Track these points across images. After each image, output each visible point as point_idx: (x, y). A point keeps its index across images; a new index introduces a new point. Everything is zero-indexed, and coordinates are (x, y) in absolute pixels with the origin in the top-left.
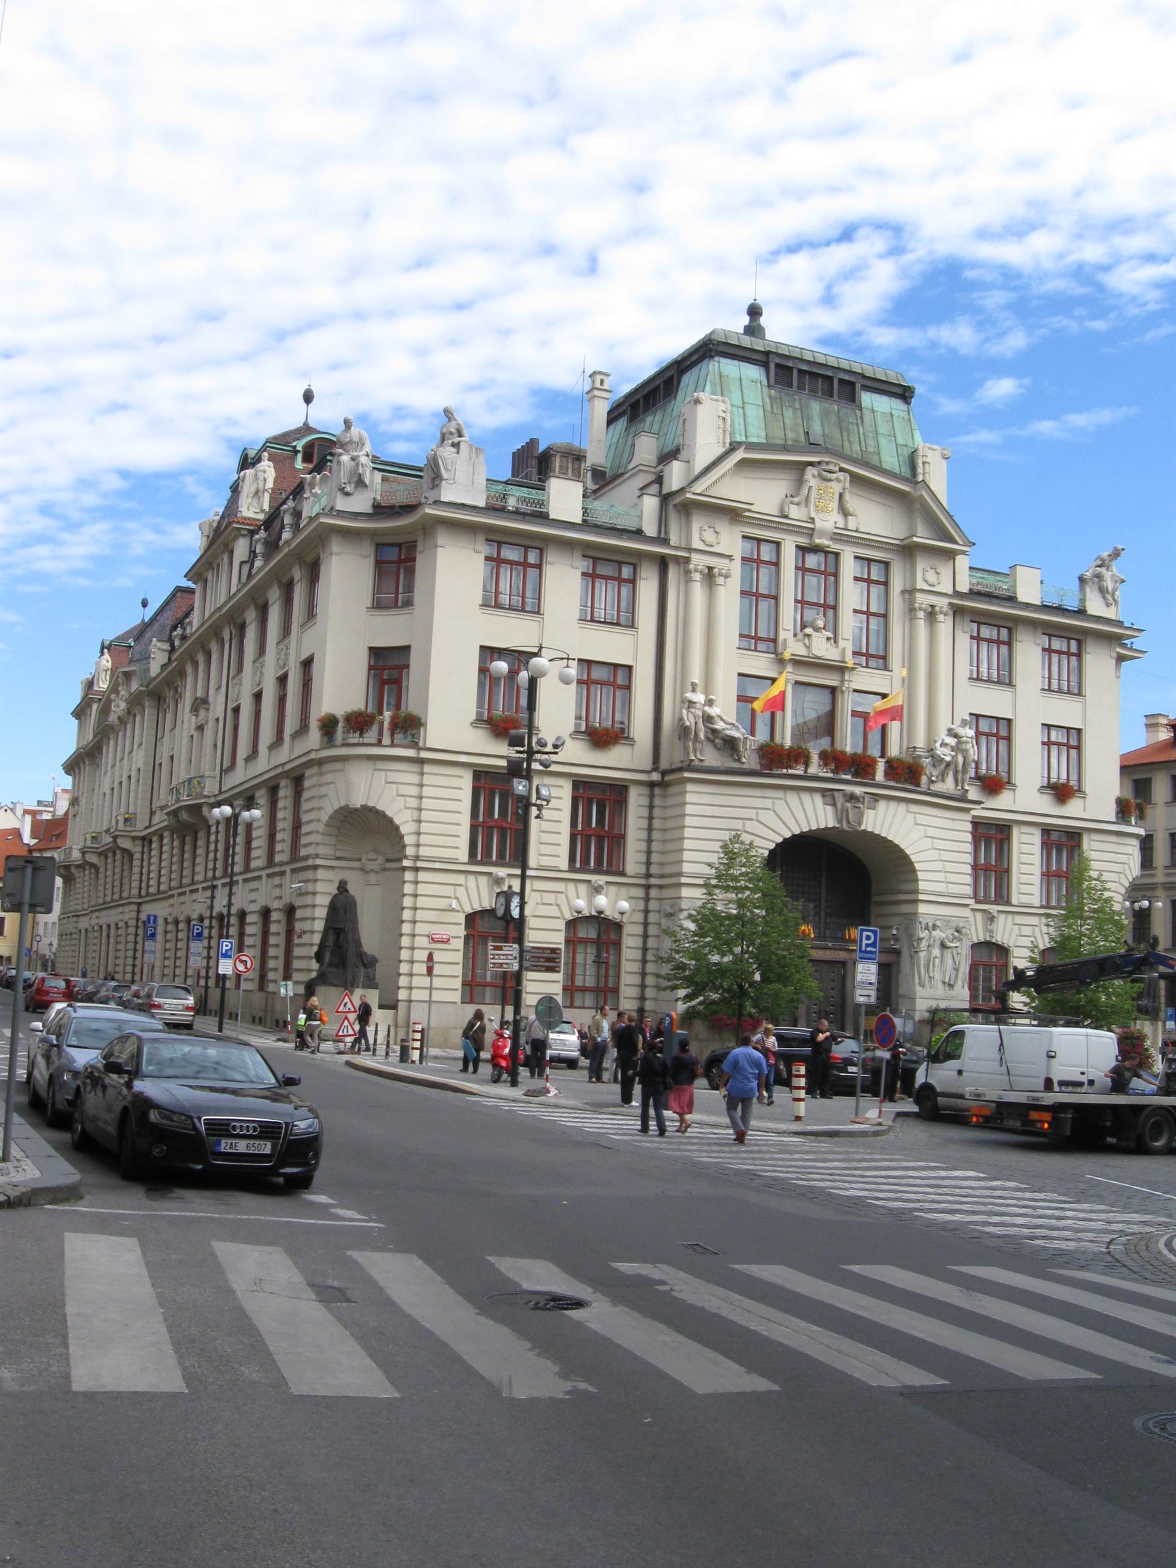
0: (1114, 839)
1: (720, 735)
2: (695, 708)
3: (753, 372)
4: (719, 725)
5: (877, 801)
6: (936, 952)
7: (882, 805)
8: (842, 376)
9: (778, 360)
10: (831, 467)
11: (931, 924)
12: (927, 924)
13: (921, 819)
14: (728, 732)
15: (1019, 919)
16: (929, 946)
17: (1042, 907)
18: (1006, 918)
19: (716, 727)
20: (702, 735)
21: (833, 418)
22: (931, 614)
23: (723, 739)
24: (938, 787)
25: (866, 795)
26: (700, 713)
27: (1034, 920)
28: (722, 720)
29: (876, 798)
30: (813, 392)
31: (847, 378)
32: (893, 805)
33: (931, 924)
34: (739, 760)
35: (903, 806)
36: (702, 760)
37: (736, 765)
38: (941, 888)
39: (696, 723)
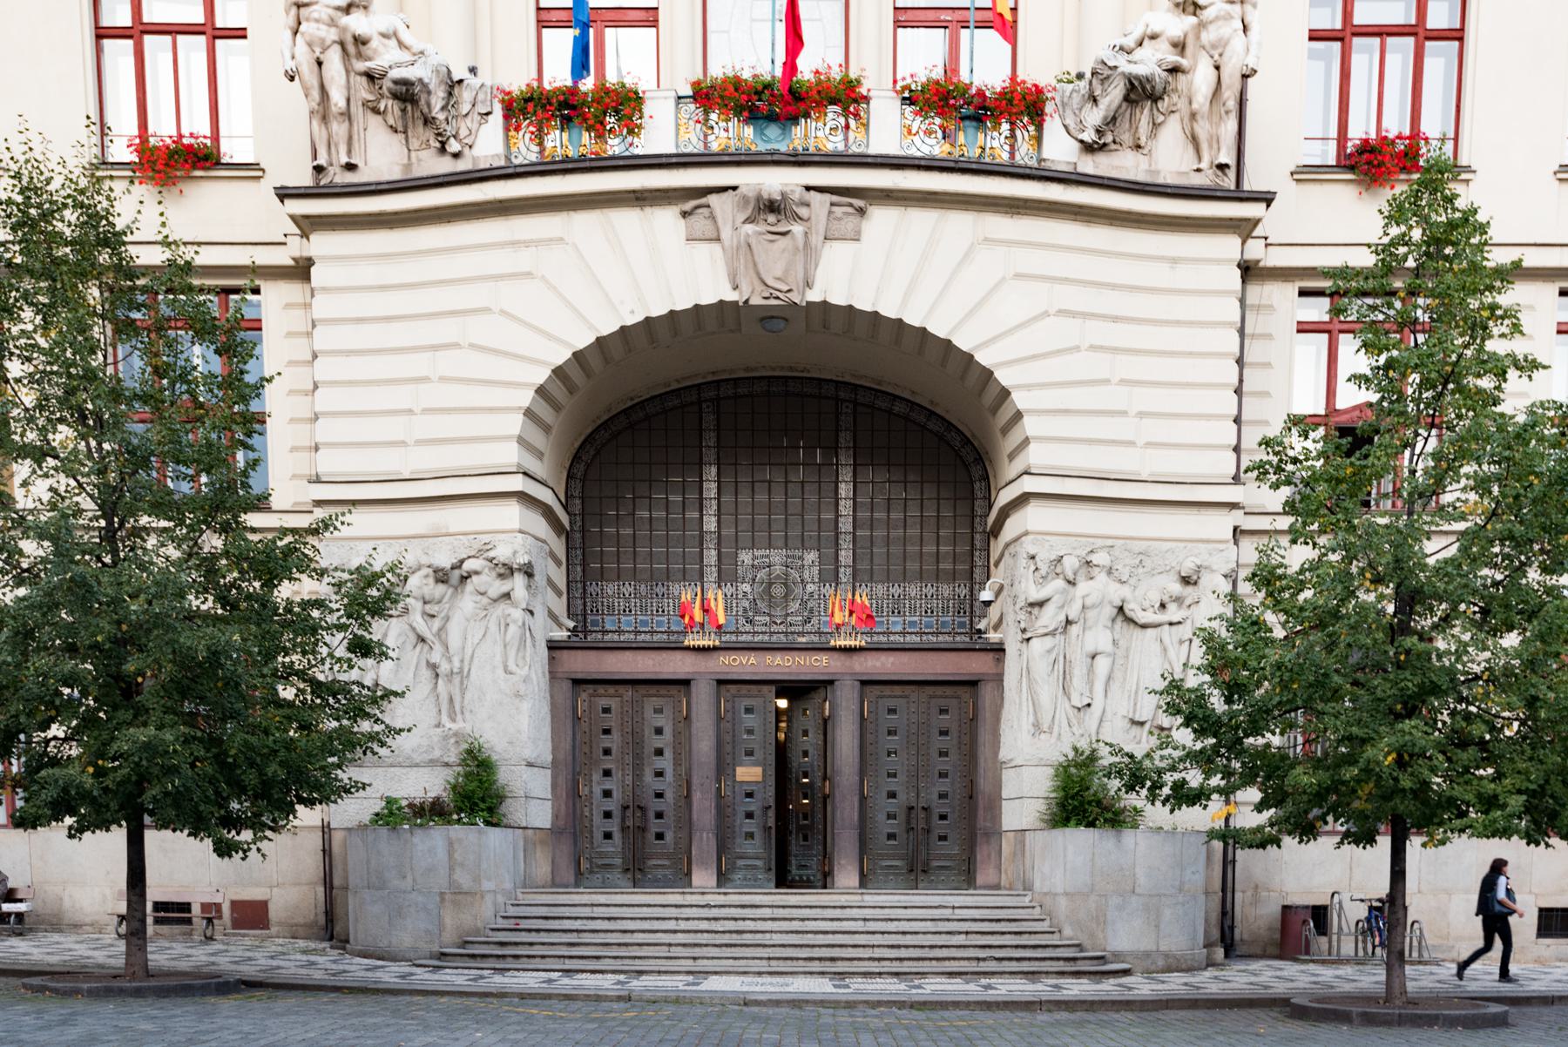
1: (387, 84)
2: (308, 20)
4: (385, 57)
6: (1099, 636)
11: (1070, 564)
12: (1060, 559)
14: (396, 74)
16: (1068, 622)
19: (369, 64)
20: (338, 99)
23: (395, 96)
26: (332, 35)
28: (401, 44)
33: (1070, 564)
34: (442, 150)
36: (351, 167)
37: (445, 166)
39: (320, 63)
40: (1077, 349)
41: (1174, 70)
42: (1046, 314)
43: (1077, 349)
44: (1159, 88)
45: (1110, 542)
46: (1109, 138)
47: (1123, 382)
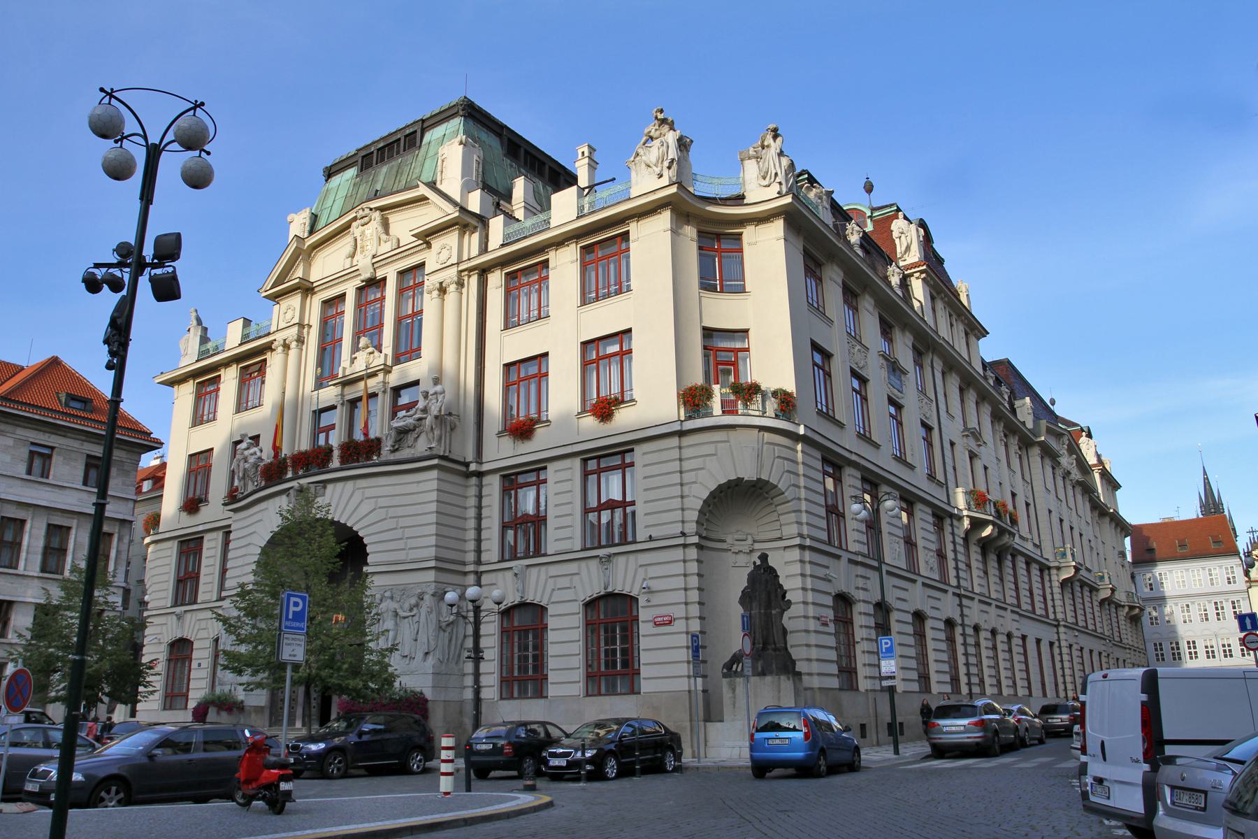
0: (674, 441)
3: (351, 172)
5: (325, 488)
7: (330, 487)
8: (408, 132)
9: (363, 153)
10: (361, 213)
13: (369, 493)
15: (554, 570)
17: (584, 549)
18: (539, 571)
21: (395, 169)
22: (442, 290)
24: (405, 453)
25: (311, 485)
26: (242, 457)
27: (573, 567)
29: (325, 483)
30: (391, 157)
31: (411, 130)
32: (340, 485)
33: (378, 596)
35: (350, 484)
38: (401, 556)
40: (385, 519)
41: (420, 419)
42: (375, 509)
43: (385, 519)
44: (411, 427)
45: (392, 588)
46: (396, 447)
47: (401, 528)
